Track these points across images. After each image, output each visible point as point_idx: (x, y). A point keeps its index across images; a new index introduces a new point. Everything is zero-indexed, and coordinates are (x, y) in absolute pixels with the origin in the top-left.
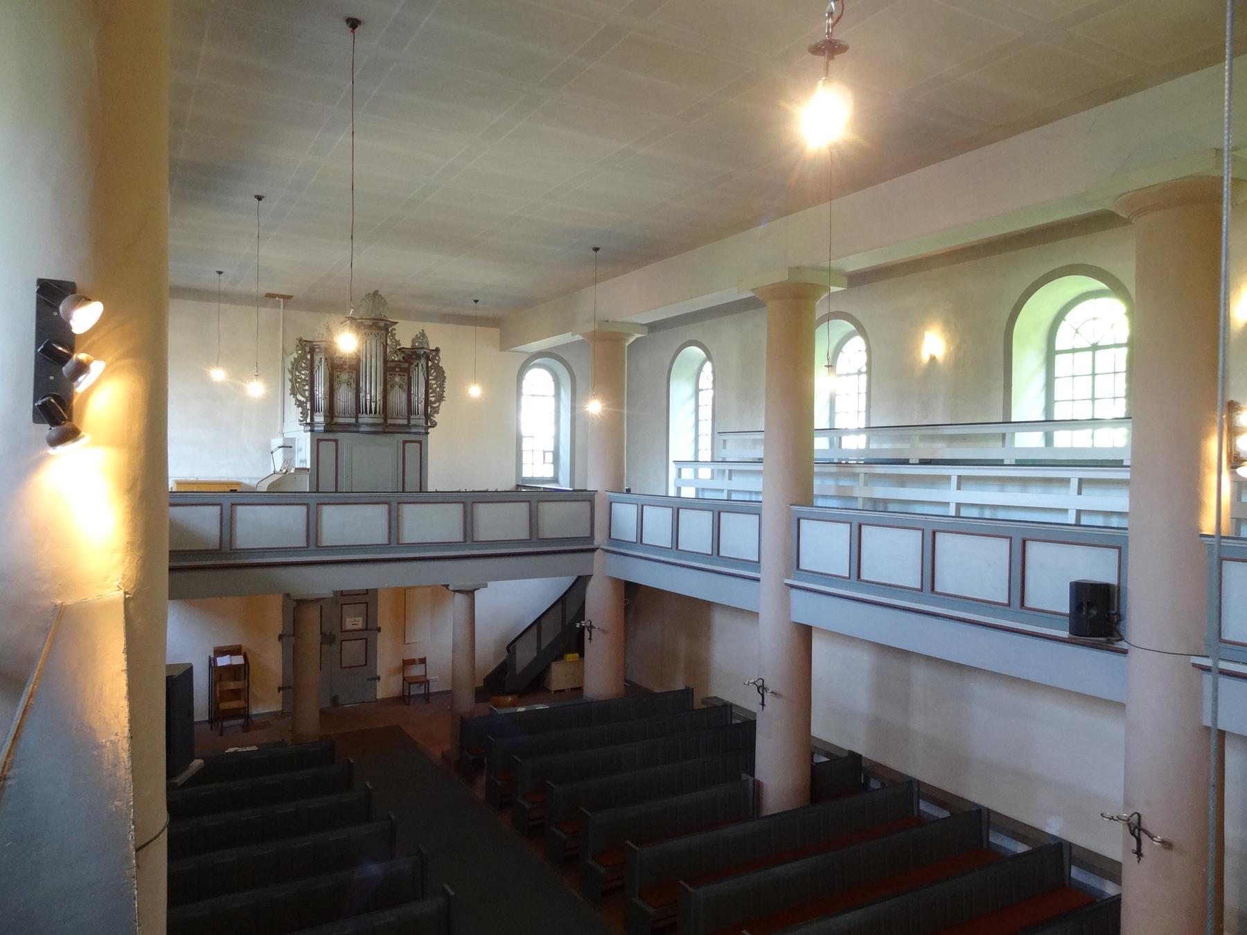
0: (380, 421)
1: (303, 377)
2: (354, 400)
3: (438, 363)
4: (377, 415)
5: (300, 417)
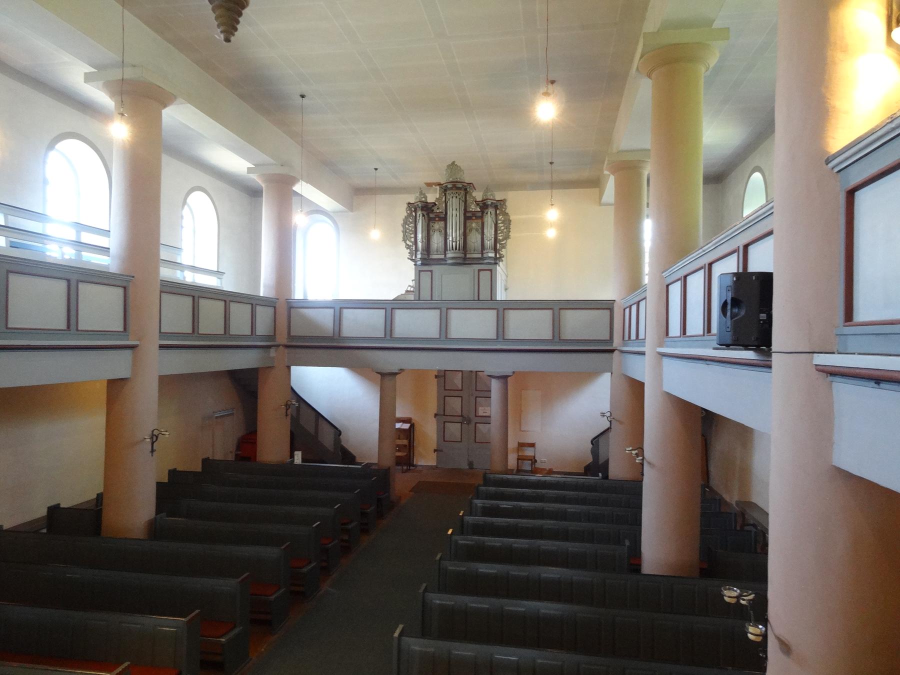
0: (463, 255)
1: (410, 228)
2: (443, 242)
3: (505, 210)
4: (457, 251)
5: (408, 255)
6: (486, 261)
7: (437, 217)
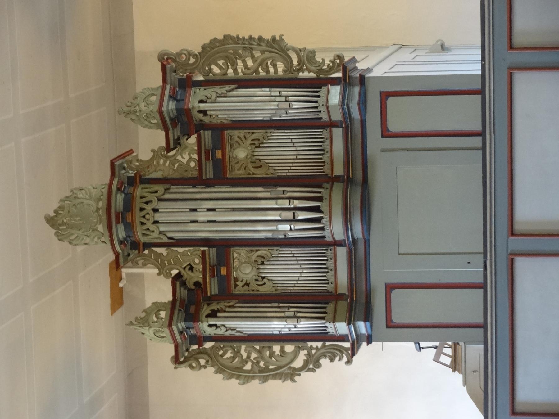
0: (338, 190)
2: (295, 251)
3: (195, 56)
4: (324, 205)
5: (339, 364)
6: (356, 114)
7: (219, 271)
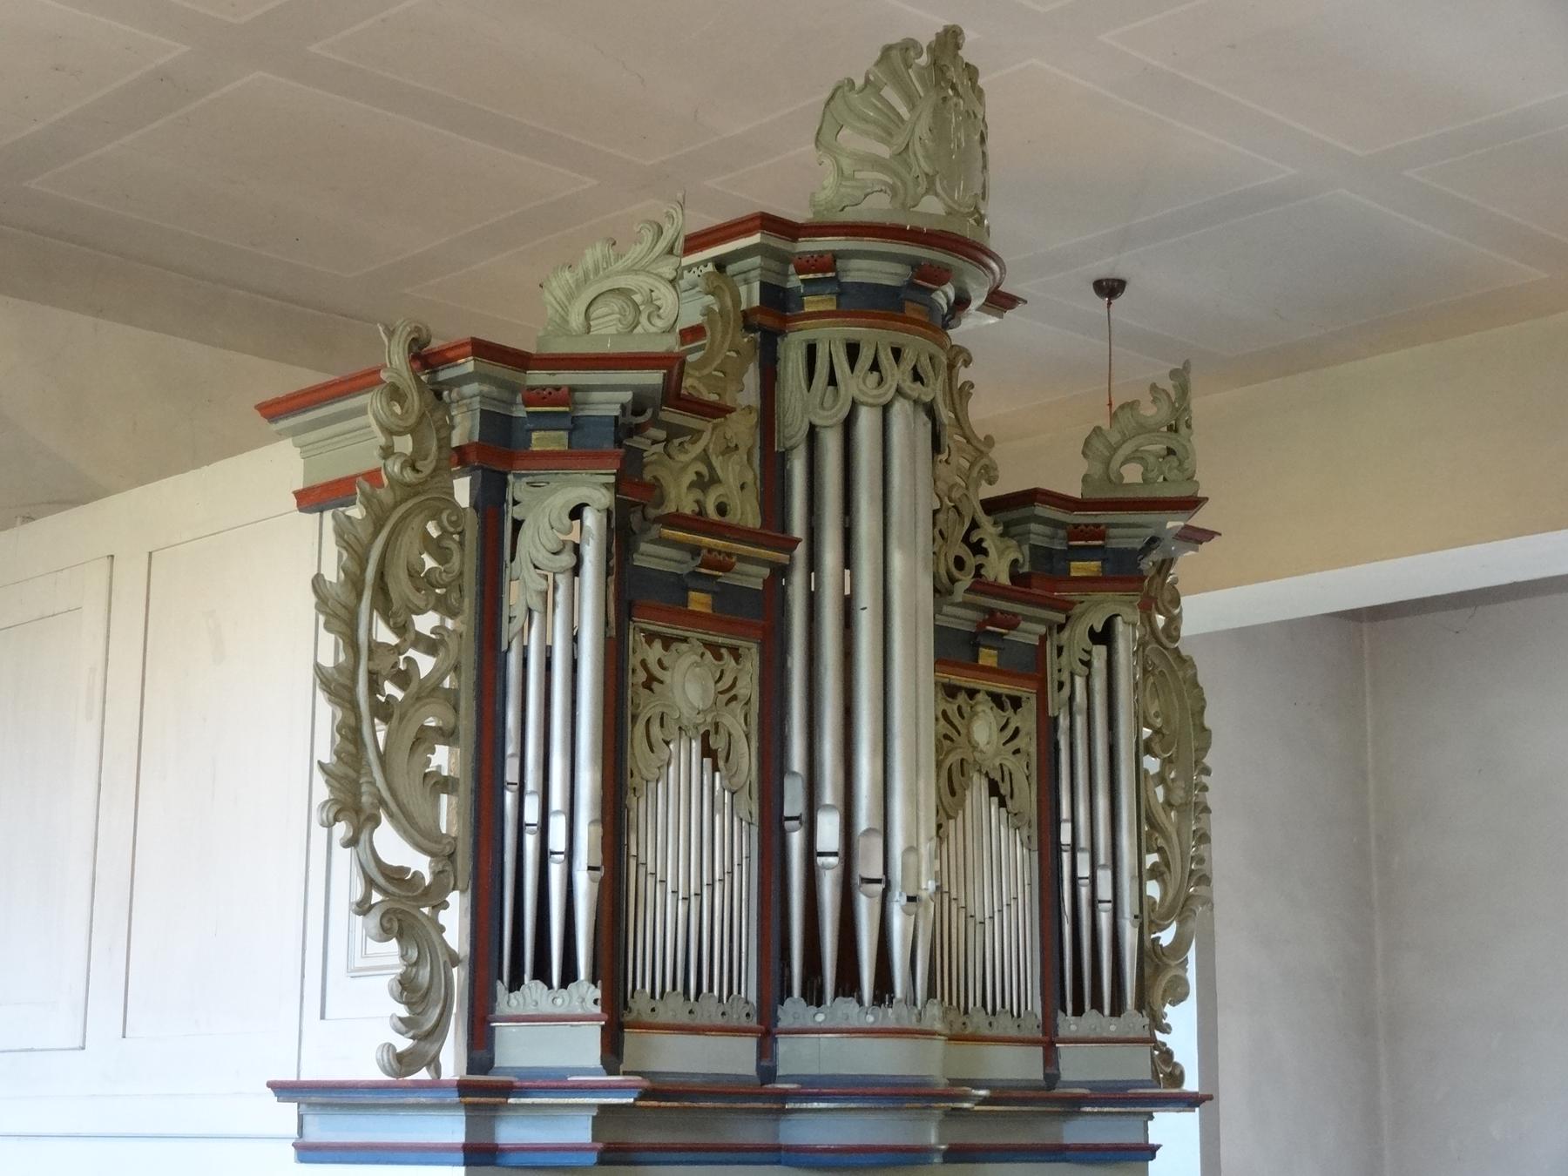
1: (426, 664)
